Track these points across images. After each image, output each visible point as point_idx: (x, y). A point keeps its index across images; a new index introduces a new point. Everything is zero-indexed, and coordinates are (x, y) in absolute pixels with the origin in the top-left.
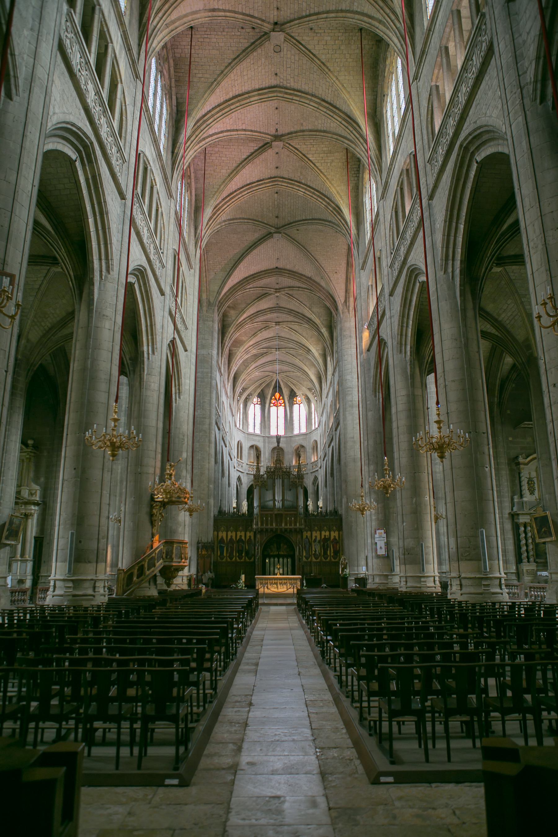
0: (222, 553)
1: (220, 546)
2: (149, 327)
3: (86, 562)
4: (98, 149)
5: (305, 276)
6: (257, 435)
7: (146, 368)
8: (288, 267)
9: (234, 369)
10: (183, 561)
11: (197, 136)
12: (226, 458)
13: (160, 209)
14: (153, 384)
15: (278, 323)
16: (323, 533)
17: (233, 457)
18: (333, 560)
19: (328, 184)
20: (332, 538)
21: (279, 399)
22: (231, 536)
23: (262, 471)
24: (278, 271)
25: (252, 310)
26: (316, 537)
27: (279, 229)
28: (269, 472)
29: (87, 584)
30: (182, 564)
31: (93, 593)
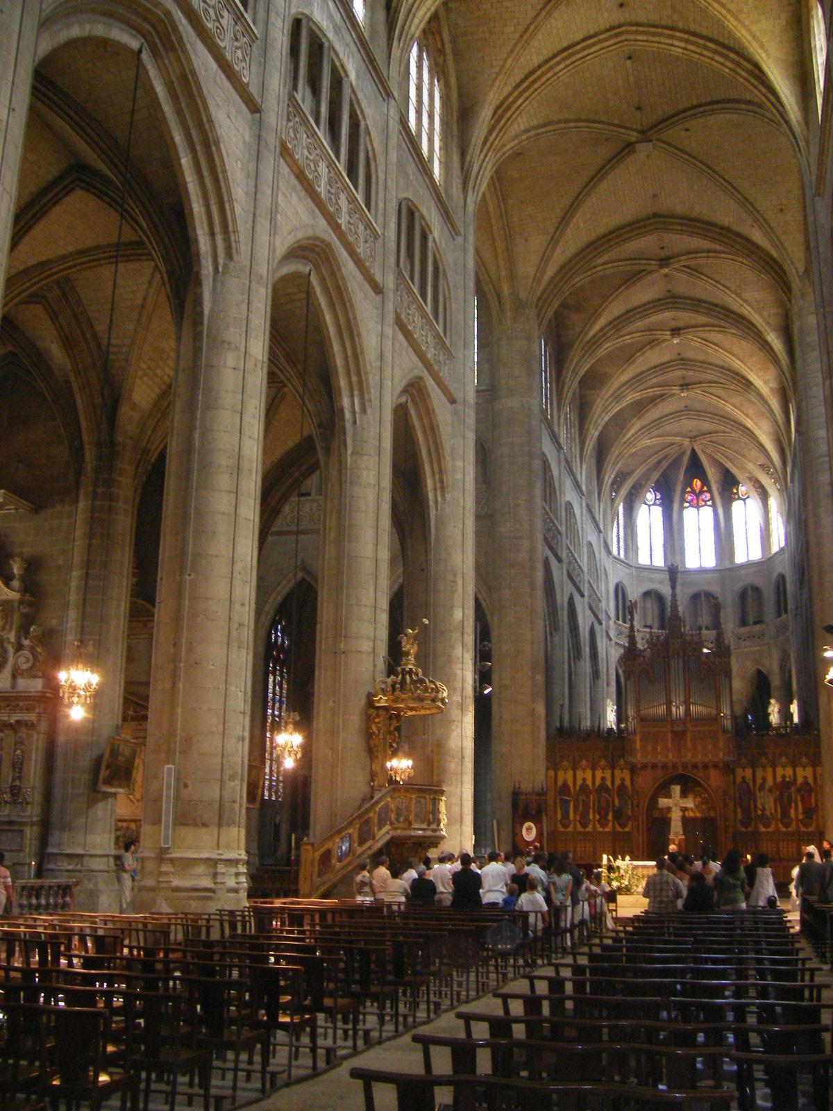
0: (565, 815)
2: (351, 359)
3: (196, 825)
4: (184, 21)
5: (714, 225)
6: (657, 570)
7: (349, 441)
8: (679, 210)
9: (594, 433)
10: (434, 826)
12: (584, 620)
13: (362, 123)
14: (364, 473)
15: (676, 331)
16: (780, 771)
17: (603, 617)
18: (803, 829)
19: (731, 23)
20: (800, 780)
21: (702, 492)
22: (584, 780)
23: (641, 645)
24: (658, 221)
25: (616, 308)
27: (646, 135)
28: (655, 645)
29: (201, 869)
30: (429, 833)
31: (211, 885)
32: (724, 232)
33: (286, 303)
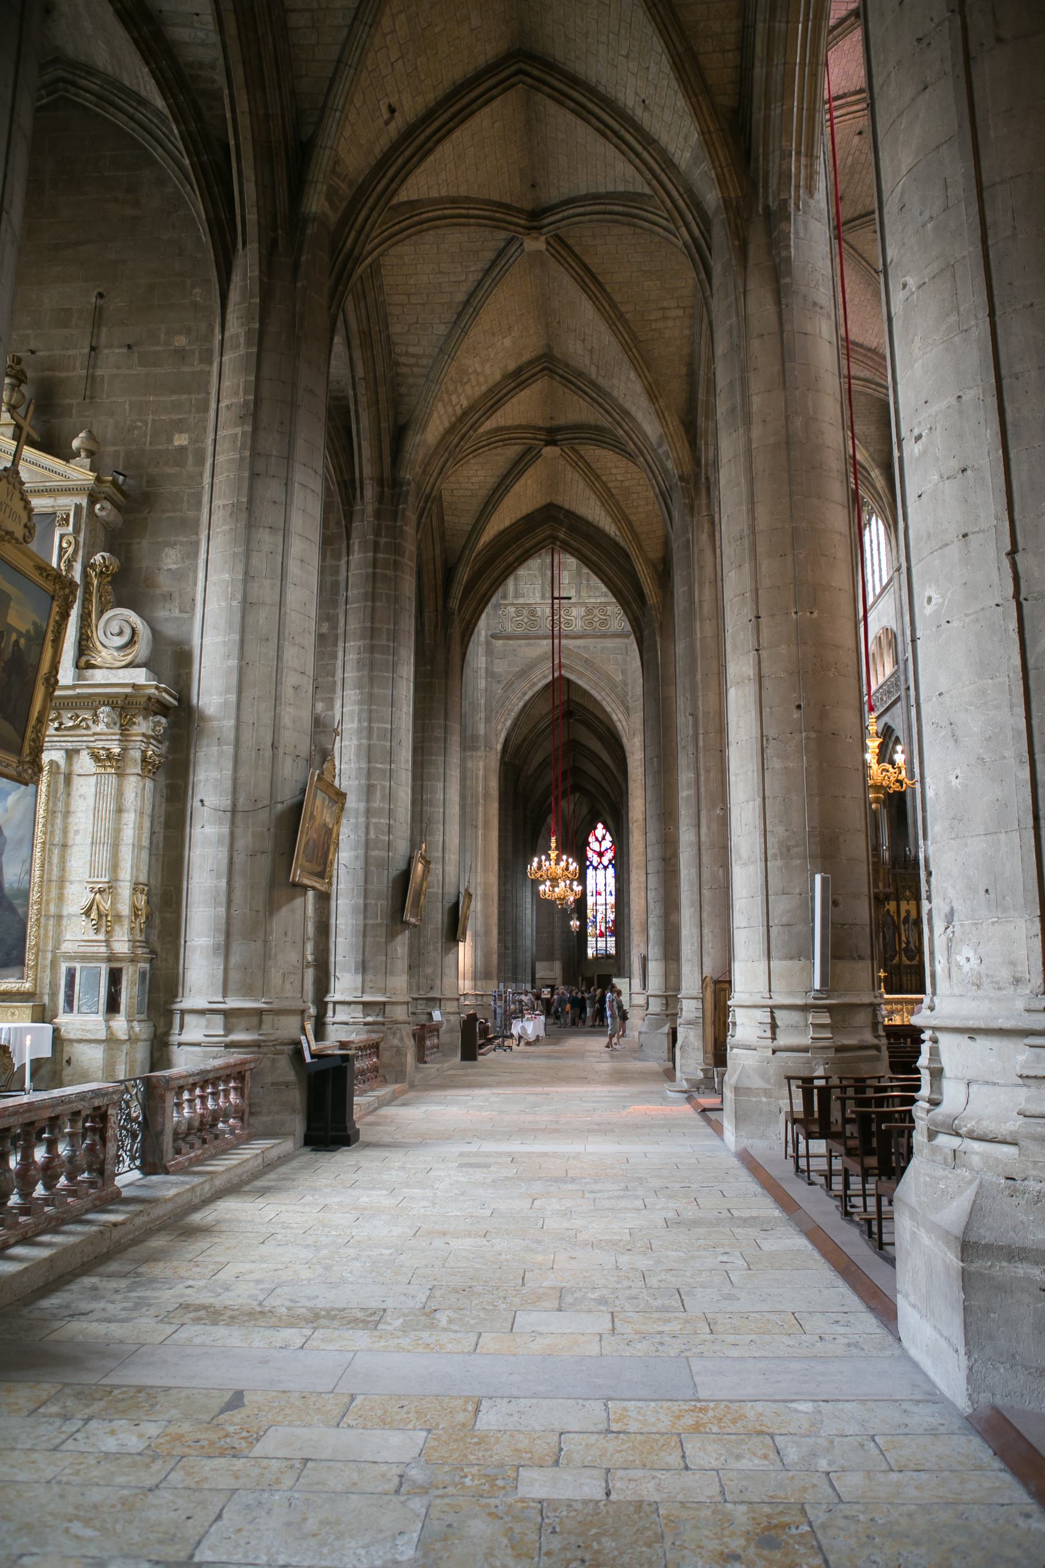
26: (908, 912)
32: (869, 354)
33: (656, 320)
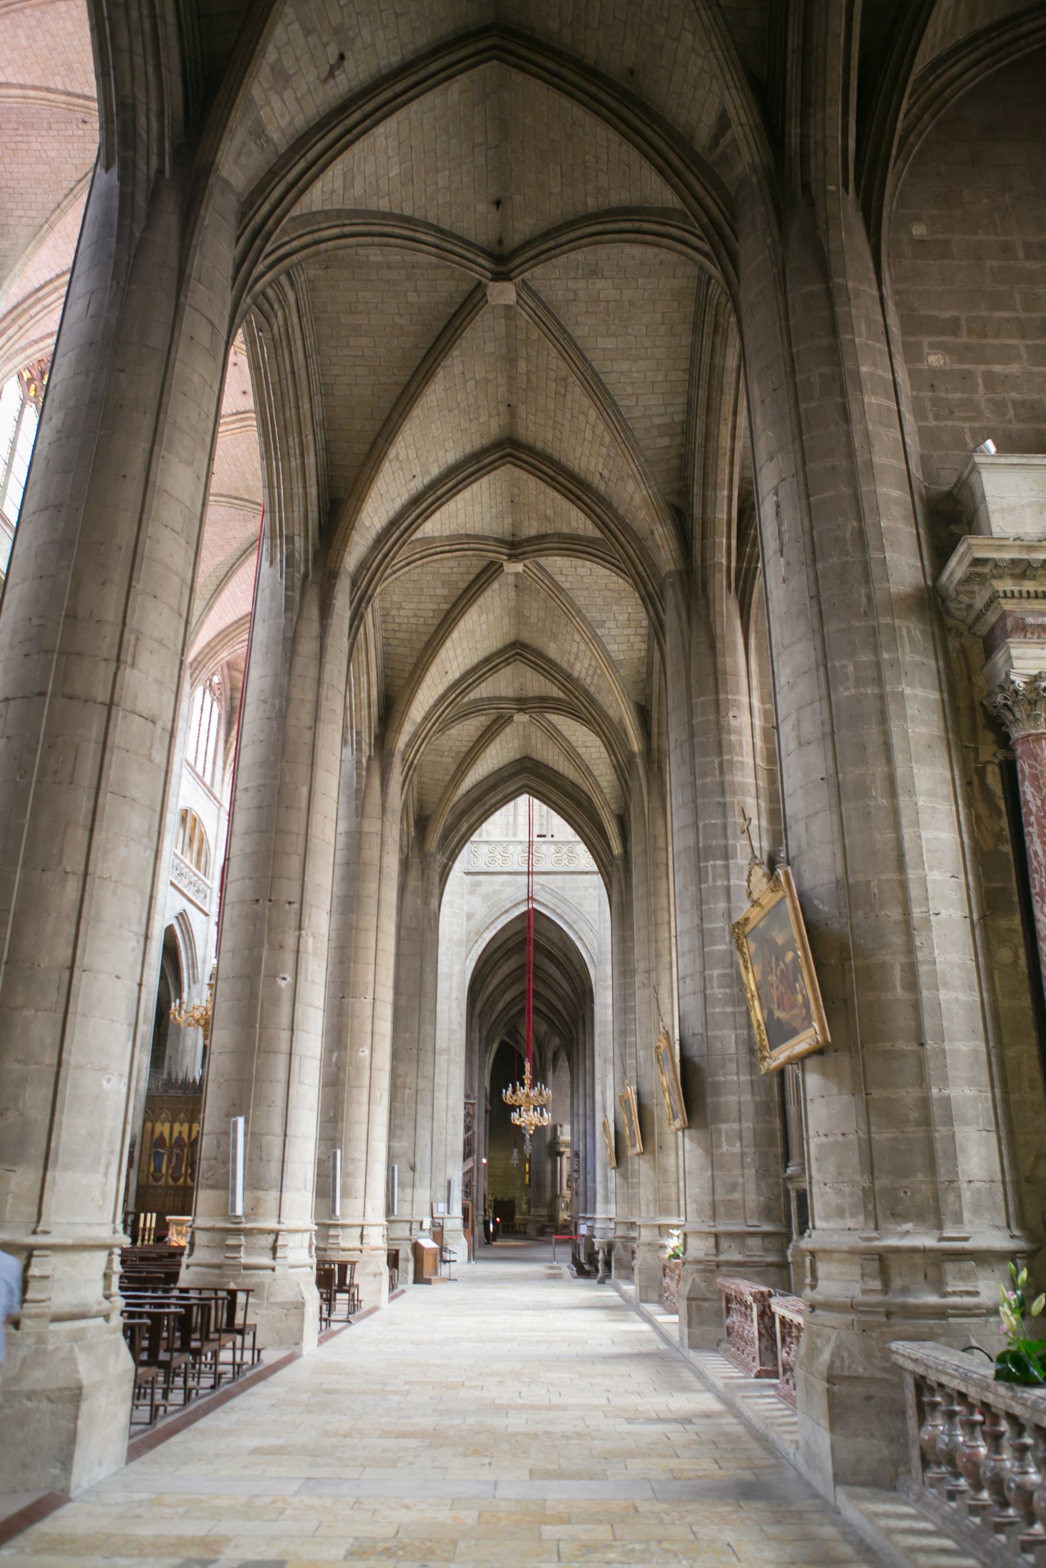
0: (158, 1169)
1: (157, 1153)
11: (21, 328)
22: (180, 1133)
